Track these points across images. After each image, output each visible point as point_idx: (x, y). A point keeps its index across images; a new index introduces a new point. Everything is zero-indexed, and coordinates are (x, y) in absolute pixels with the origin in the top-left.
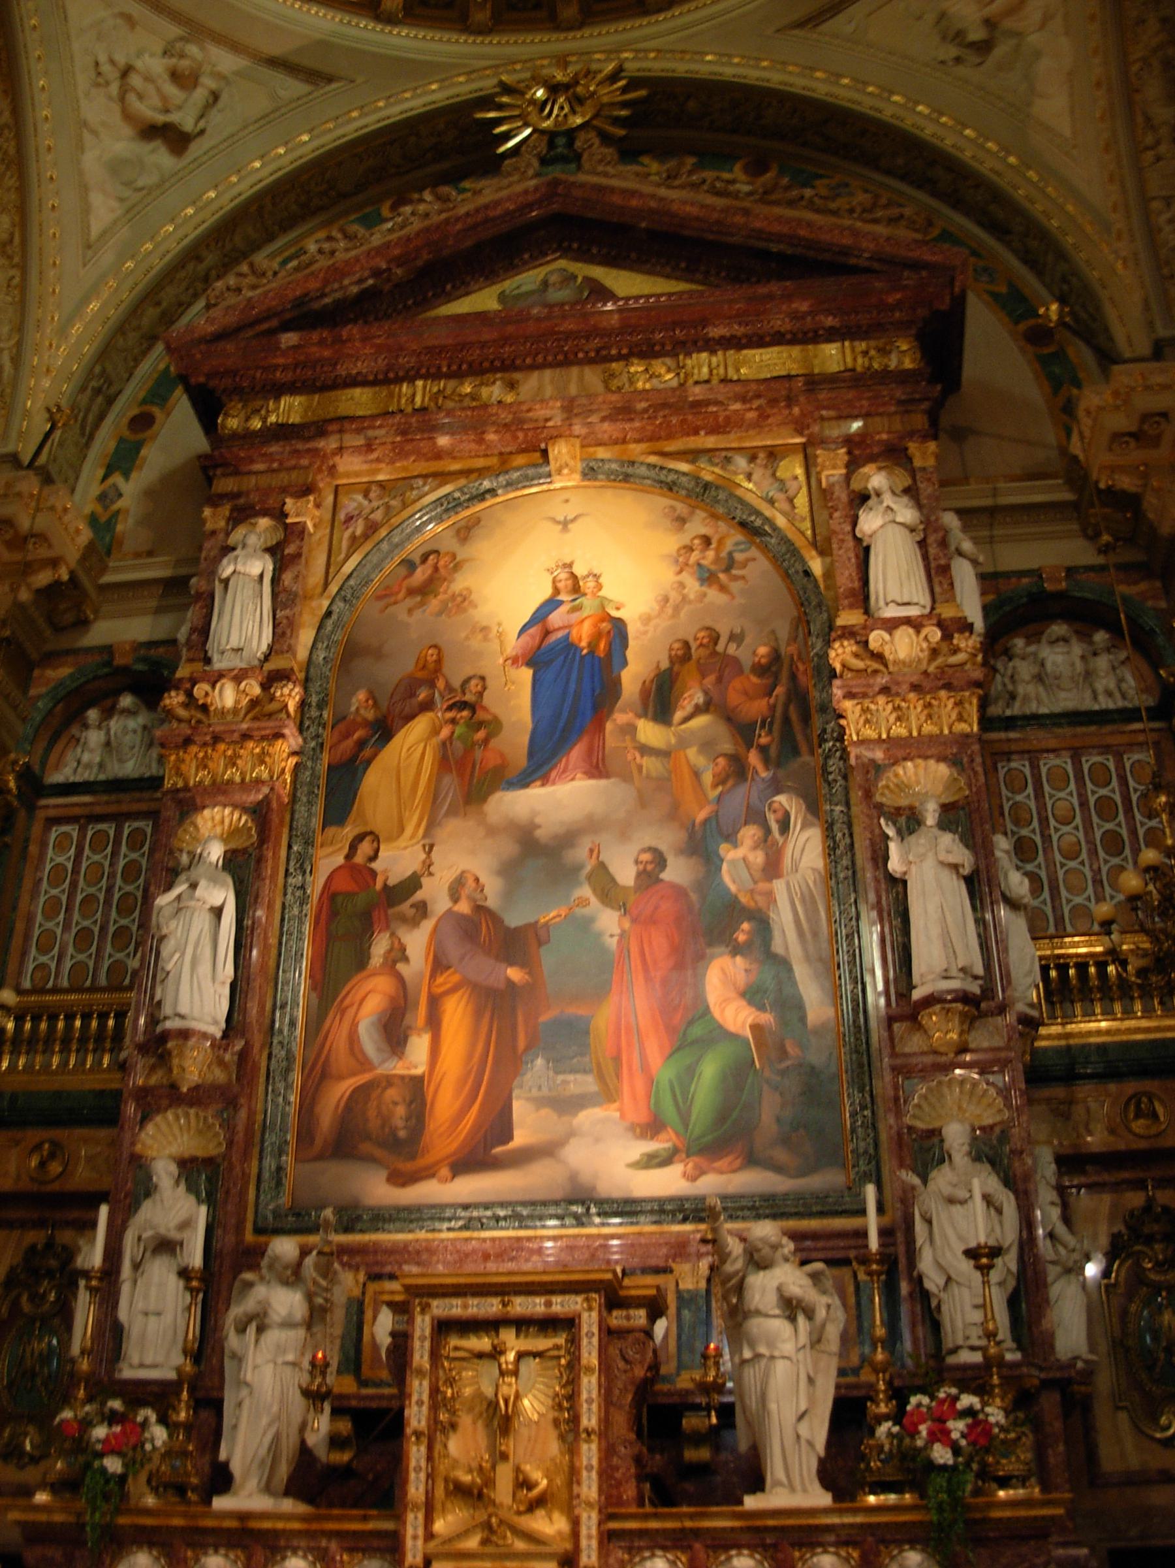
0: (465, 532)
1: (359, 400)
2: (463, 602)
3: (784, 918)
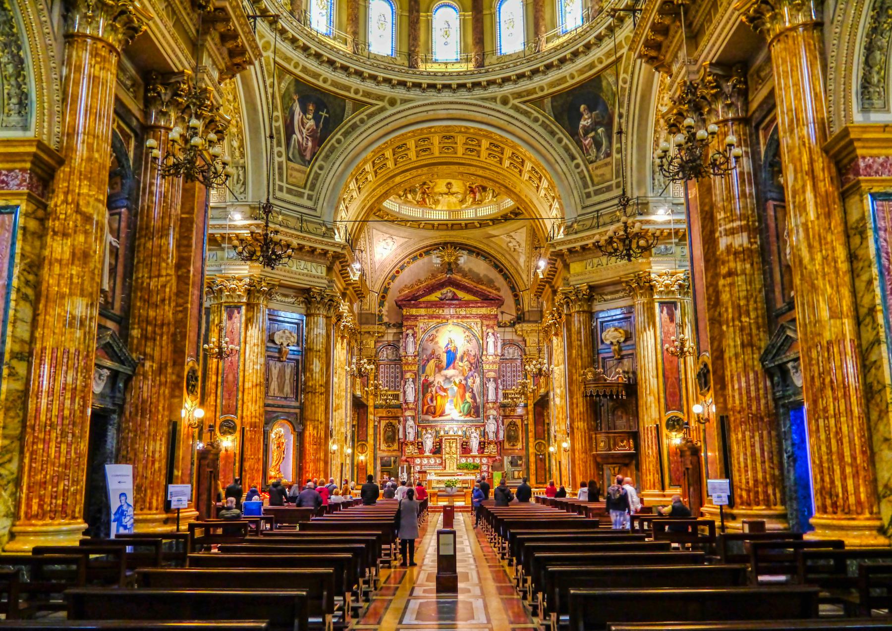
0: (437, 332)
1: (422, 311)
2: (437, 343)
3: (475, 389)
